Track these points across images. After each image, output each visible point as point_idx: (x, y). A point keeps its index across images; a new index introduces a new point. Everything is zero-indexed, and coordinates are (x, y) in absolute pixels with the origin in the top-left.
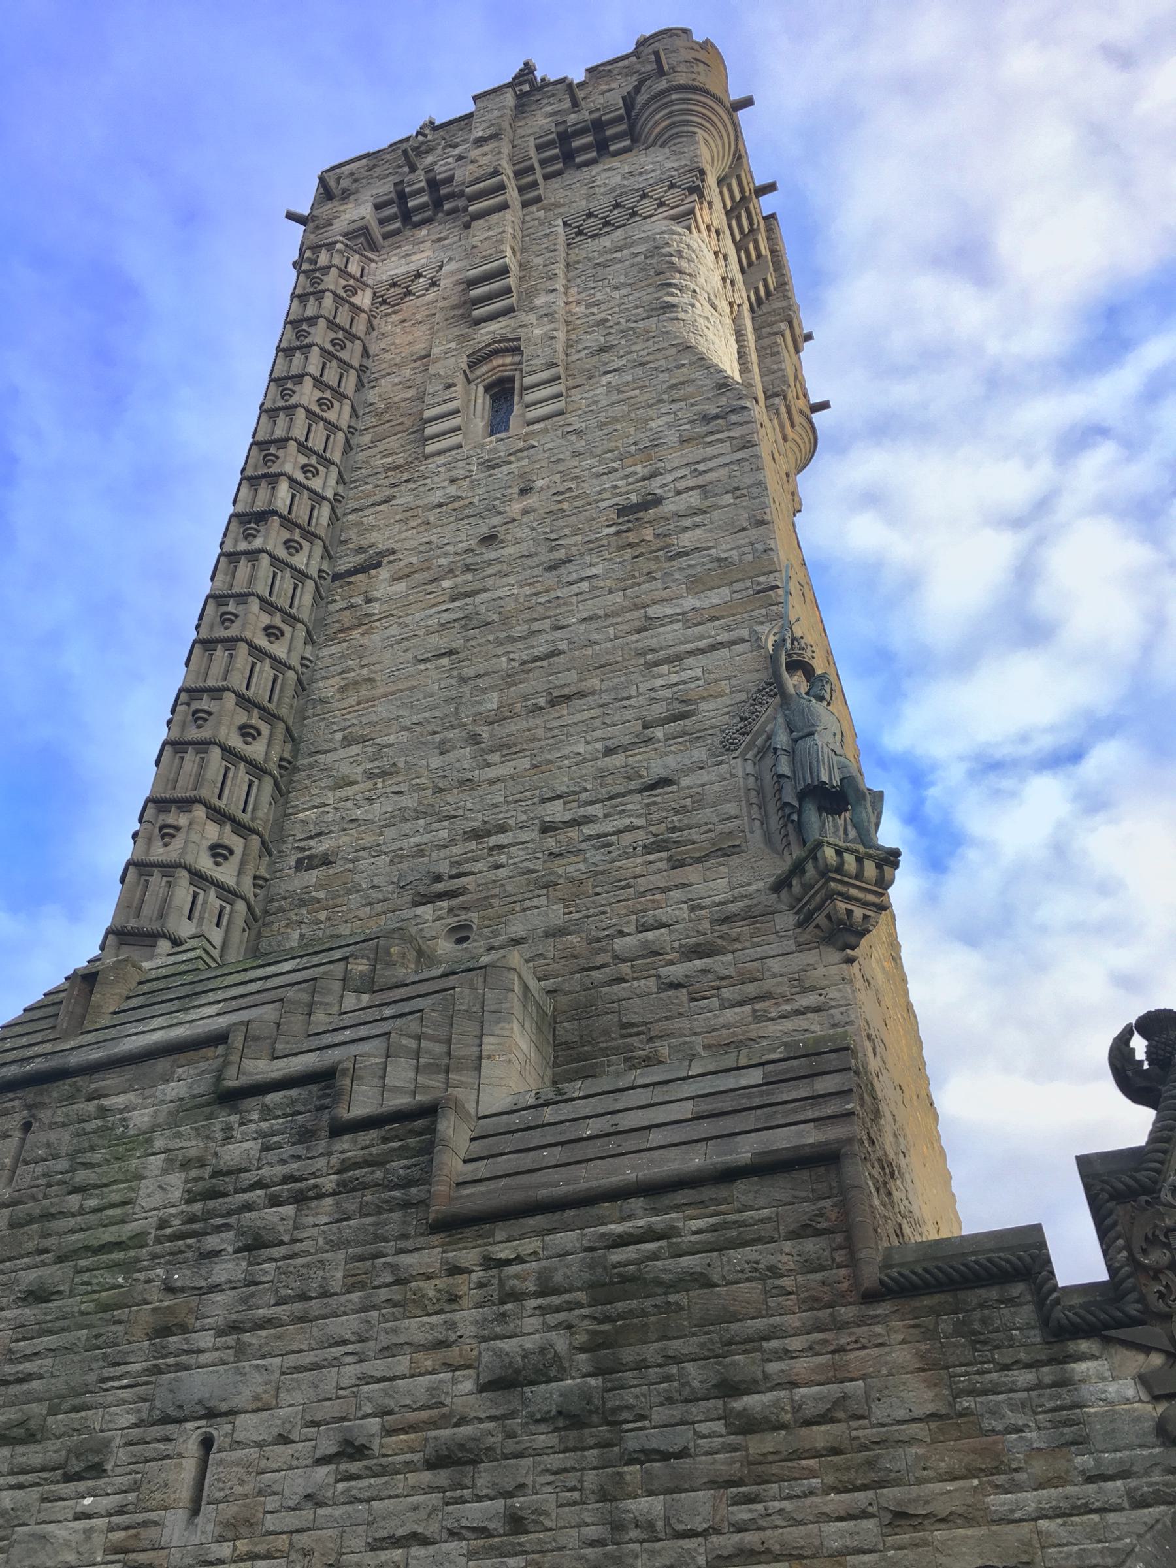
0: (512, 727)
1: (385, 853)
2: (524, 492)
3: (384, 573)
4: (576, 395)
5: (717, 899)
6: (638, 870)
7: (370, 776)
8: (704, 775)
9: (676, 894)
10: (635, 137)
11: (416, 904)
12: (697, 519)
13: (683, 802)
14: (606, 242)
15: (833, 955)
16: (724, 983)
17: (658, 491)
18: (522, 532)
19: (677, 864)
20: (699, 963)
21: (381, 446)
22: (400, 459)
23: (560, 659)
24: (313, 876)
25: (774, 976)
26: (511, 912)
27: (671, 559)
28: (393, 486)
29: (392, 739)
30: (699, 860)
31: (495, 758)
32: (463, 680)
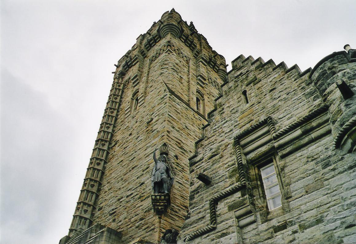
0: (127, 175)
1: (108, 206)
2: (136, 122)
3: (117, 145)
4: (146, 98)
5: (145, 208)
6: (137, 203)
7: (109, 190)
8: (148, 181)
9: (141, 208)
10: (160, 38)
11: (110, 216)
12: (156, 123)
13: (144, 187)
14: (156, 61)
15: (157, 217)
16: (143, 225)
17: (153, 117)
18: (135, 131)
19: (142, 201)
20: (141, 222)
21: (121, 117)
22: (122, 120)
23: (135, 159)
24: (99, 212)
25: (150, 223)
26: (121, 215)
27: (152, 132)
28: (121, 126)
29: (112, 181)
30: (145, 199)
31: (124, 182)
32: (123, 166)
